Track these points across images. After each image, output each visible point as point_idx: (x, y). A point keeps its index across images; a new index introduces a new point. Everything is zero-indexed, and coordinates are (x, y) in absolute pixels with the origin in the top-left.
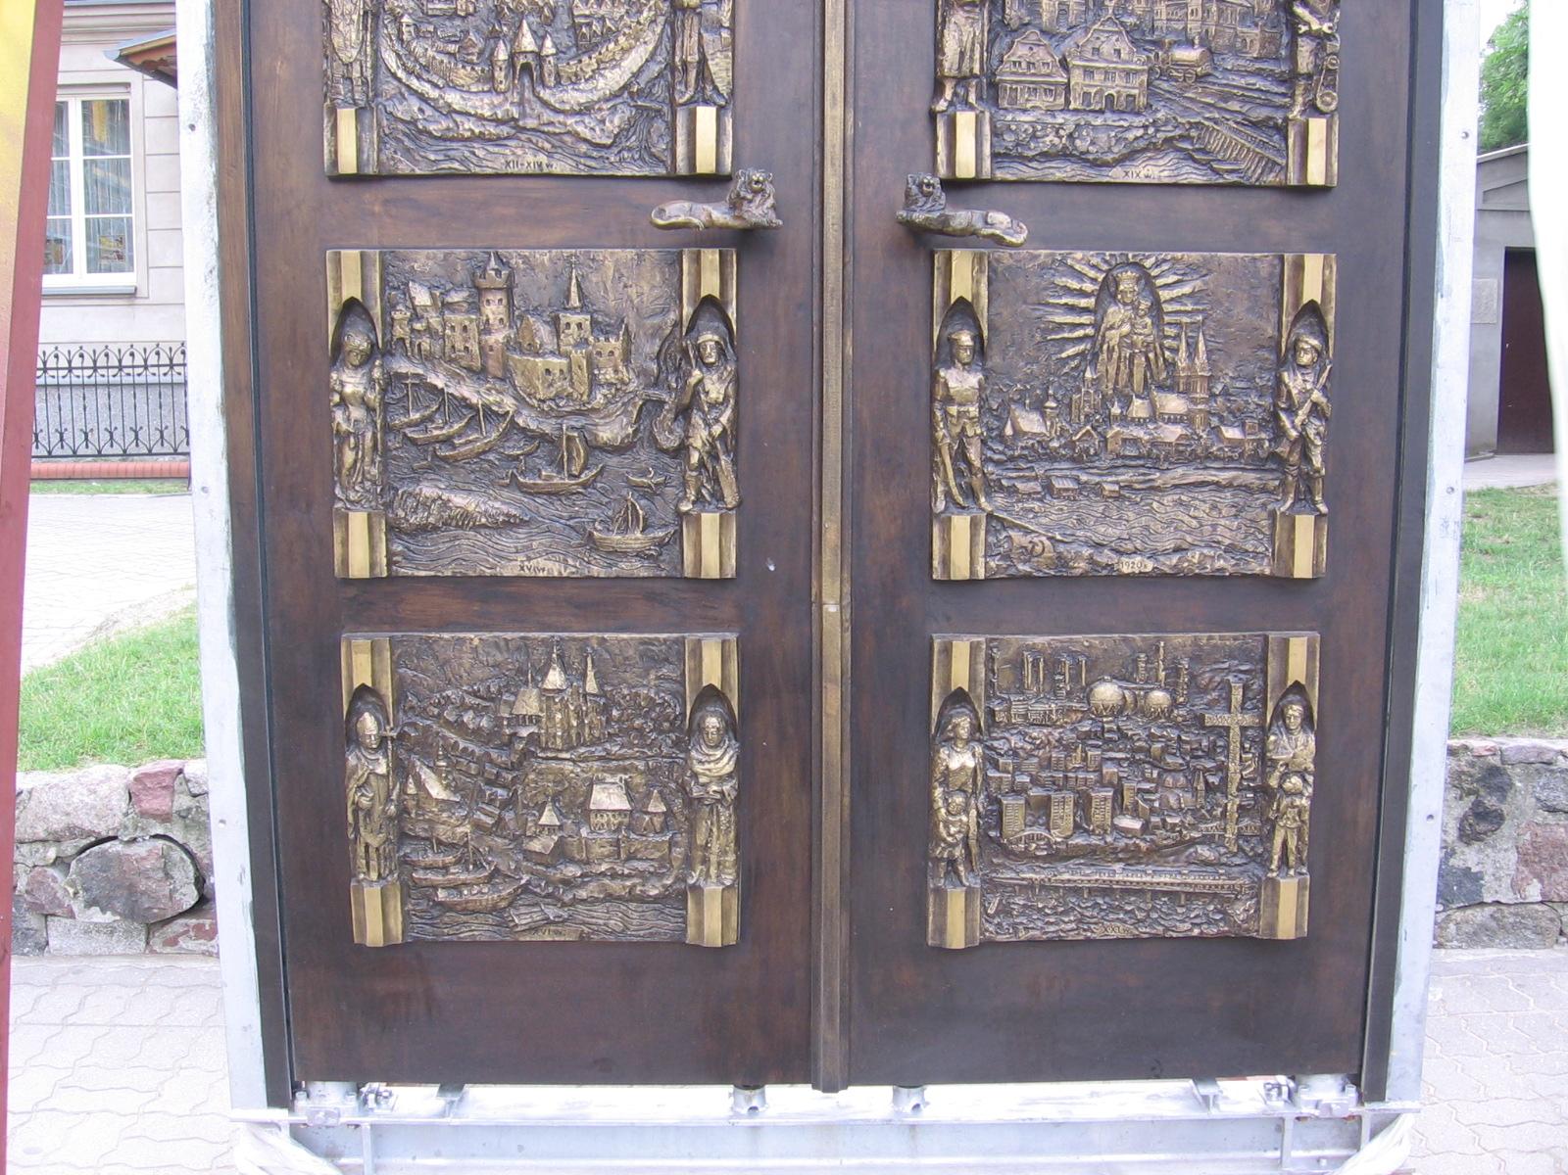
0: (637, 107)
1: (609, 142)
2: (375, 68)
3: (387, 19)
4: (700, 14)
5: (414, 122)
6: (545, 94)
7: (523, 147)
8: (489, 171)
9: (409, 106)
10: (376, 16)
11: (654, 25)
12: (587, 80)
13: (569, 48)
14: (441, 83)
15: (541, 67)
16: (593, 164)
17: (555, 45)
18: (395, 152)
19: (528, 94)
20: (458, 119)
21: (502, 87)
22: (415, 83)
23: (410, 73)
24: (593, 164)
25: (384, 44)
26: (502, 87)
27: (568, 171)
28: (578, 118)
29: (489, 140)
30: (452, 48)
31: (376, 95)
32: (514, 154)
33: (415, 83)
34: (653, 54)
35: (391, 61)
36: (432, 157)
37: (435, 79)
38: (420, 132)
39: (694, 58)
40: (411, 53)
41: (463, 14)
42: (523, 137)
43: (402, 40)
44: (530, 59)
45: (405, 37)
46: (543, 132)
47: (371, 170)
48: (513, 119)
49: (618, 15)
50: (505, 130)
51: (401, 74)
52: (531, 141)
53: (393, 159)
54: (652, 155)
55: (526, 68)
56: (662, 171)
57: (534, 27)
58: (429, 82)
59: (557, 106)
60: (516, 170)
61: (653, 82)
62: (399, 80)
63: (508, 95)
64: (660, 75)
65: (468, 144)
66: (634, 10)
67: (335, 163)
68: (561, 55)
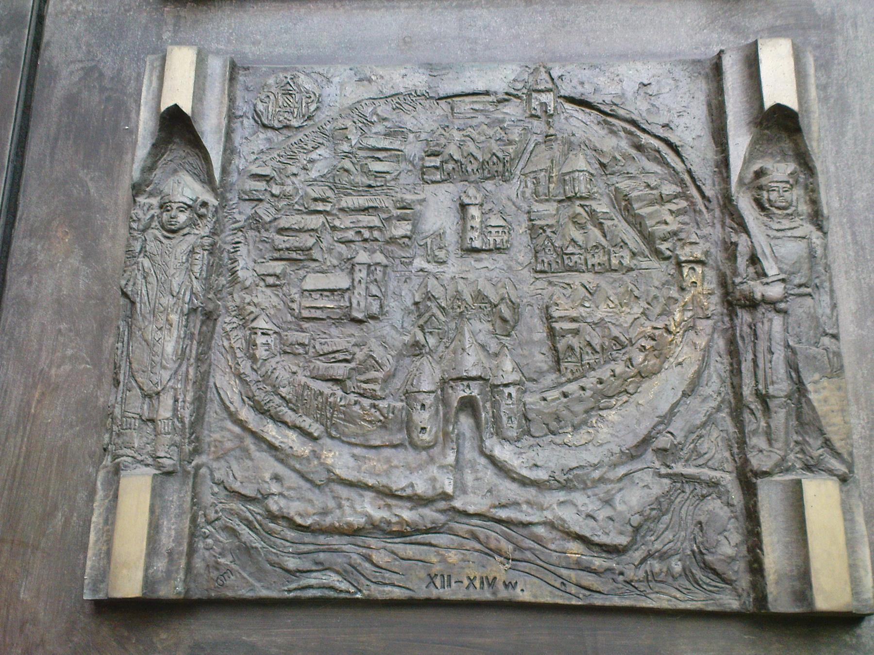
0: (674, 477)
1: (623, 540)
2: (200, 402)
3: (226, 322)
4: (785, 312)
5: (261, 498)
6: (504, 452)
7: (459, 548)
8: (397, 593)
9: (256, 469)
10: (210, 317)
11: (691, 333)
12: (576, 428)
13: (542, 373)
14: (316, 429)
15: (495, 404)
16: (589, 580)
17: (518, 367)
18: (222, 554)
19: (470, 453)
20: (343, 492)
21: (426, 437)
22: (272, 432)
23: (261, 410)
24: (589, 580)
25: (218, 358)
26: (426, 437)
27: (547, 596)
28: (562, 496)
29: (401, 534)
30: (340, 370)
31: (196, 451)
32: (443, 560)
33: (272, 432)
34: (692, 389)
35: (231, 391)
36: (292, 563)
37: (307, 423)
38: (273, 517)
39: (781, 387)
40: (266, 377)
41: (360, 316)
42: (462, 528)
43: (253, 358)
44: (475, 390)
45: (261, 353)
46: (500, 521)
47: (166, 592)
48: (446, 497)
49: (630, 319)
50: (429, 515)
51: (246, 414)
52: (476, 538)
53: (217, 566)
54: (708, 568)
55: (469, 405)
56: (733, 604)
57: (481, 338)
58: (295, 427)
59: (525, 472)
60: (447, 594)
61: (696, 431)
62: (242, 424)
63: (436, 450)
64: (710, 421)
65: (359, 540)
66: (658, 310)
67: (103, 575)
68: (529, 384)
